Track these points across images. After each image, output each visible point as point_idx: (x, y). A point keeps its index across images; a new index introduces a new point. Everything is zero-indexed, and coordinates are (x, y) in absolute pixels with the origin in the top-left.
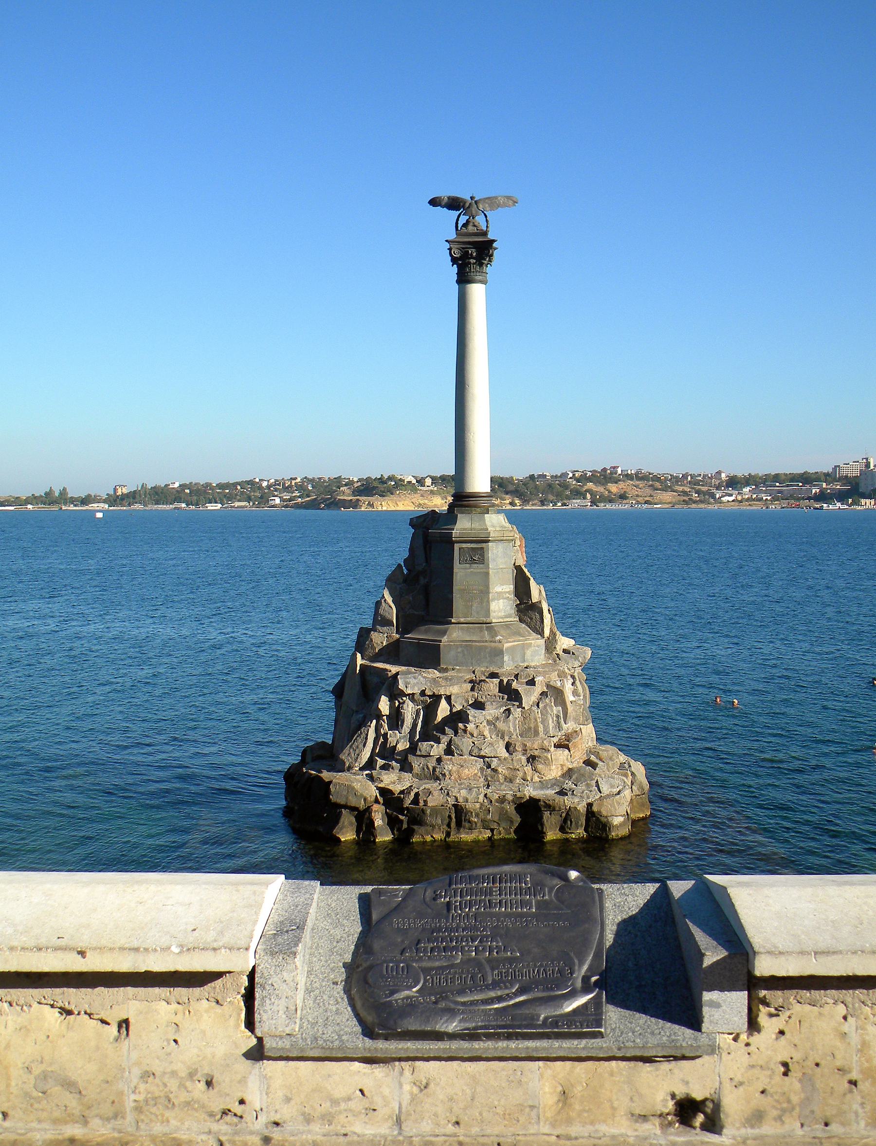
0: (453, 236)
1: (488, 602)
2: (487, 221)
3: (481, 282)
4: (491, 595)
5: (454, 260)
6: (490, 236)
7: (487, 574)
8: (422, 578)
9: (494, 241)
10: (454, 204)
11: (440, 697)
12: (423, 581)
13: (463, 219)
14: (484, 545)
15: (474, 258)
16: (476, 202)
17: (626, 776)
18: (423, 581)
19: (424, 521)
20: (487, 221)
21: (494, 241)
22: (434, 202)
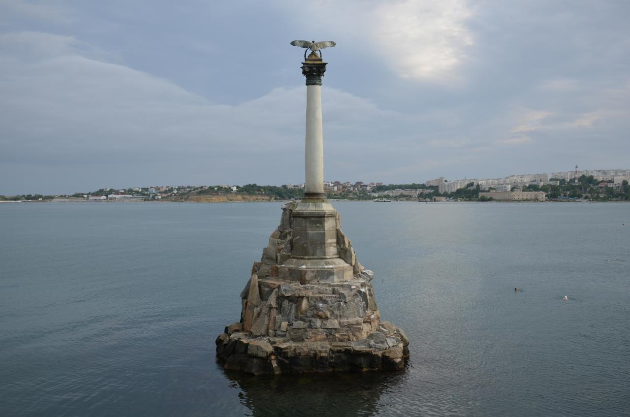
0: (304, 61)
1: (325, 248)
2: (321, 53)
3: (318, 84)
4: (326, 245)
5: (304, 73)
6: (324, 61)
7: (324, 233)
8: (288, 236)
9: (326, 64)
10: (306, 45)
11: (302, 297)
12: (289, 238)
13: (309, 52)
14: (322, 219)
15: (316, 72)
16: (316, 44)
17: (398, 336)
18: (289, 238)
19: (290, 206)
20: (321, 53)
21: (326, 64)
22: (293, 43)
